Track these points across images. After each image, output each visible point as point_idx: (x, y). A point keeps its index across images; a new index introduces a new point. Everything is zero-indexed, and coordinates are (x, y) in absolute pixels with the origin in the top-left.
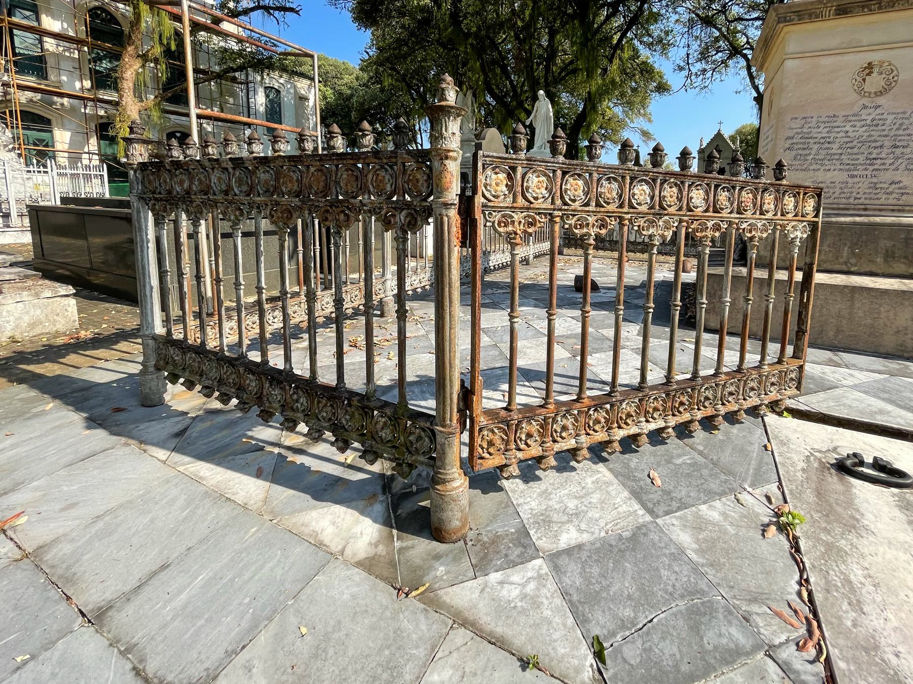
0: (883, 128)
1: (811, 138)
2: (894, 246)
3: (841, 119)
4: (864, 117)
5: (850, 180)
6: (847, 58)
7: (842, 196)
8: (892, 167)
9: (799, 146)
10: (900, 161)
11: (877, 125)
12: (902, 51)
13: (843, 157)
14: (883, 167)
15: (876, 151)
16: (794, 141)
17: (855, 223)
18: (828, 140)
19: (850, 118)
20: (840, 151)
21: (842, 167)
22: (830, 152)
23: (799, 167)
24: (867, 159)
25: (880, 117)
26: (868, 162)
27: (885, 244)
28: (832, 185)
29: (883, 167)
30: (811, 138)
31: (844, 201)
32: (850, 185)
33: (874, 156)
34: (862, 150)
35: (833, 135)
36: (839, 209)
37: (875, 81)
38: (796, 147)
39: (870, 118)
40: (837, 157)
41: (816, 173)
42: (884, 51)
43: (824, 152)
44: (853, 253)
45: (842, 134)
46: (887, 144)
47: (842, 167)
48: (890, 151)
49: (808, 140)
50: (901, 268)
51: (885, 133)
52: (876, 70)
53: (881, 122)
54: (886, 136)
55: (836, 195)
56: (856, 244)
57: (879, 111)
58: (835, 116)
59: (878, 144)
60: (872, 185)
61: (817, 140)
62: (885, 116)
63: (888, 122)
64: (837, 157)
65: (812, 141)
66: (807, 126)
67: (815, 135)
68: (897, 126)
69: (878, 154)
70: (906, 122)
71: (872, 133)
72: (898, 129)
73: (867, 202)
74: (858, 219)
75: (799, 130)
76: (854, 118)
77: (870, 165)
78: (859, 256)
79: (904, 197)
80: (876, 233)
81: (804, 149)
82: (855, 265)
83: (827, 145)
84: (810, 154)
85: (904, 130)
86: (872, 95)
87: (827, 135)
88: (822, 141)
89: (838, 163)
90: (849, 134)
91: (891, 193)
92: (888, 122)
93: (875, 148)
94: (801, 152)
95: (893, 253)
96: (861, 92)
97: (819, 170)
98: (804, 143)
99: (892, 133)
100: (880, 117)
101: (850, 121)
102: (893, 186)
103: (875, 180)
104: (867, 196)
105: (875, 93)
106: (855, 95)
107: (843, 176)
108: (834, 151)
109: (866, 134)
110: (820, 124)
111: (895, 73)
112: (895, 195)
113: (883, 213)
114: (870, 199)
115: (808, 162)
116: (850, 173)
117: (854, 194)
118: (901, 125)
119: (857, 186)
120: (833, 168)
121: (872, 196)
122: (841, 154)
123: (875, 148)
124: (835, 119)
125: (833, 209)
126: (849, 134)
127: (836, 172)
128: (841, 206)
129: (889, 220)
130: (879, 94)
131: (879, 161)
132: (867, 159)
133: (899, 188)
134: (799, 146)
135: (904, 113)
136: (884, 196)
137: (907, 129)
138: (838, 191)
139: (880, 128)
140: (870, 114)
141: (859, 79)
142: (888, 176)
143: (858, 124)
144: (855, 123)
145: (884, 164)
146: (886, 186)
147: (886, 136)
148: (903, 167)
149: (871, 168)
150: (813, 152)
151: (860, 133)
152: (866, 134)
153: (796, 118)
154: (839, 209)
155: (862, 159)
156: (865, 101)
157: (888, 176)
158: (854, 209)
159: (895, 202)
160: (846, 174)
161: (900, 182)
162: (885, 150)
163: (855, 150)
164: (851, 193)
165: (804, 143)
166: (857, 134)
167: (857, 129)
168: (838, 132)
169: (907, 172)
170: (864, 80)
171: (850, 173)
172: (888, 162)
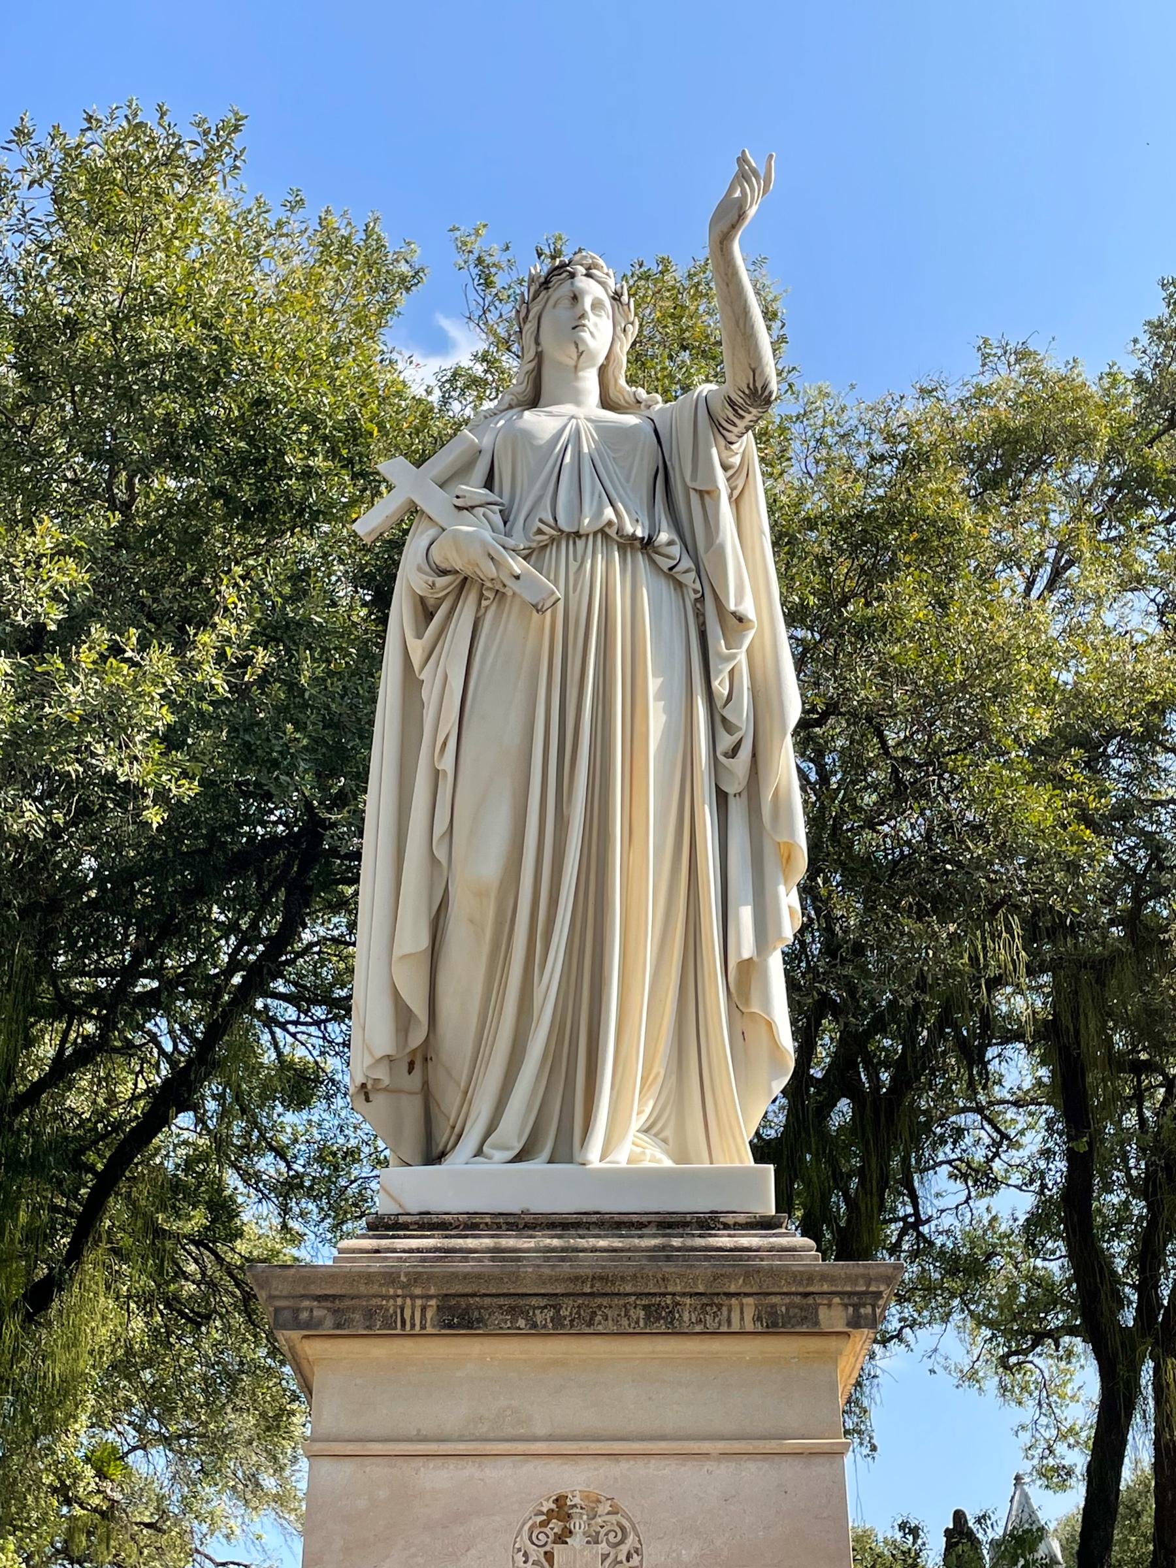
42: (592, 1463)
52: (579, 1524)
111: (631, 1540)
141: (536, 1554)
170: (549, 1556)
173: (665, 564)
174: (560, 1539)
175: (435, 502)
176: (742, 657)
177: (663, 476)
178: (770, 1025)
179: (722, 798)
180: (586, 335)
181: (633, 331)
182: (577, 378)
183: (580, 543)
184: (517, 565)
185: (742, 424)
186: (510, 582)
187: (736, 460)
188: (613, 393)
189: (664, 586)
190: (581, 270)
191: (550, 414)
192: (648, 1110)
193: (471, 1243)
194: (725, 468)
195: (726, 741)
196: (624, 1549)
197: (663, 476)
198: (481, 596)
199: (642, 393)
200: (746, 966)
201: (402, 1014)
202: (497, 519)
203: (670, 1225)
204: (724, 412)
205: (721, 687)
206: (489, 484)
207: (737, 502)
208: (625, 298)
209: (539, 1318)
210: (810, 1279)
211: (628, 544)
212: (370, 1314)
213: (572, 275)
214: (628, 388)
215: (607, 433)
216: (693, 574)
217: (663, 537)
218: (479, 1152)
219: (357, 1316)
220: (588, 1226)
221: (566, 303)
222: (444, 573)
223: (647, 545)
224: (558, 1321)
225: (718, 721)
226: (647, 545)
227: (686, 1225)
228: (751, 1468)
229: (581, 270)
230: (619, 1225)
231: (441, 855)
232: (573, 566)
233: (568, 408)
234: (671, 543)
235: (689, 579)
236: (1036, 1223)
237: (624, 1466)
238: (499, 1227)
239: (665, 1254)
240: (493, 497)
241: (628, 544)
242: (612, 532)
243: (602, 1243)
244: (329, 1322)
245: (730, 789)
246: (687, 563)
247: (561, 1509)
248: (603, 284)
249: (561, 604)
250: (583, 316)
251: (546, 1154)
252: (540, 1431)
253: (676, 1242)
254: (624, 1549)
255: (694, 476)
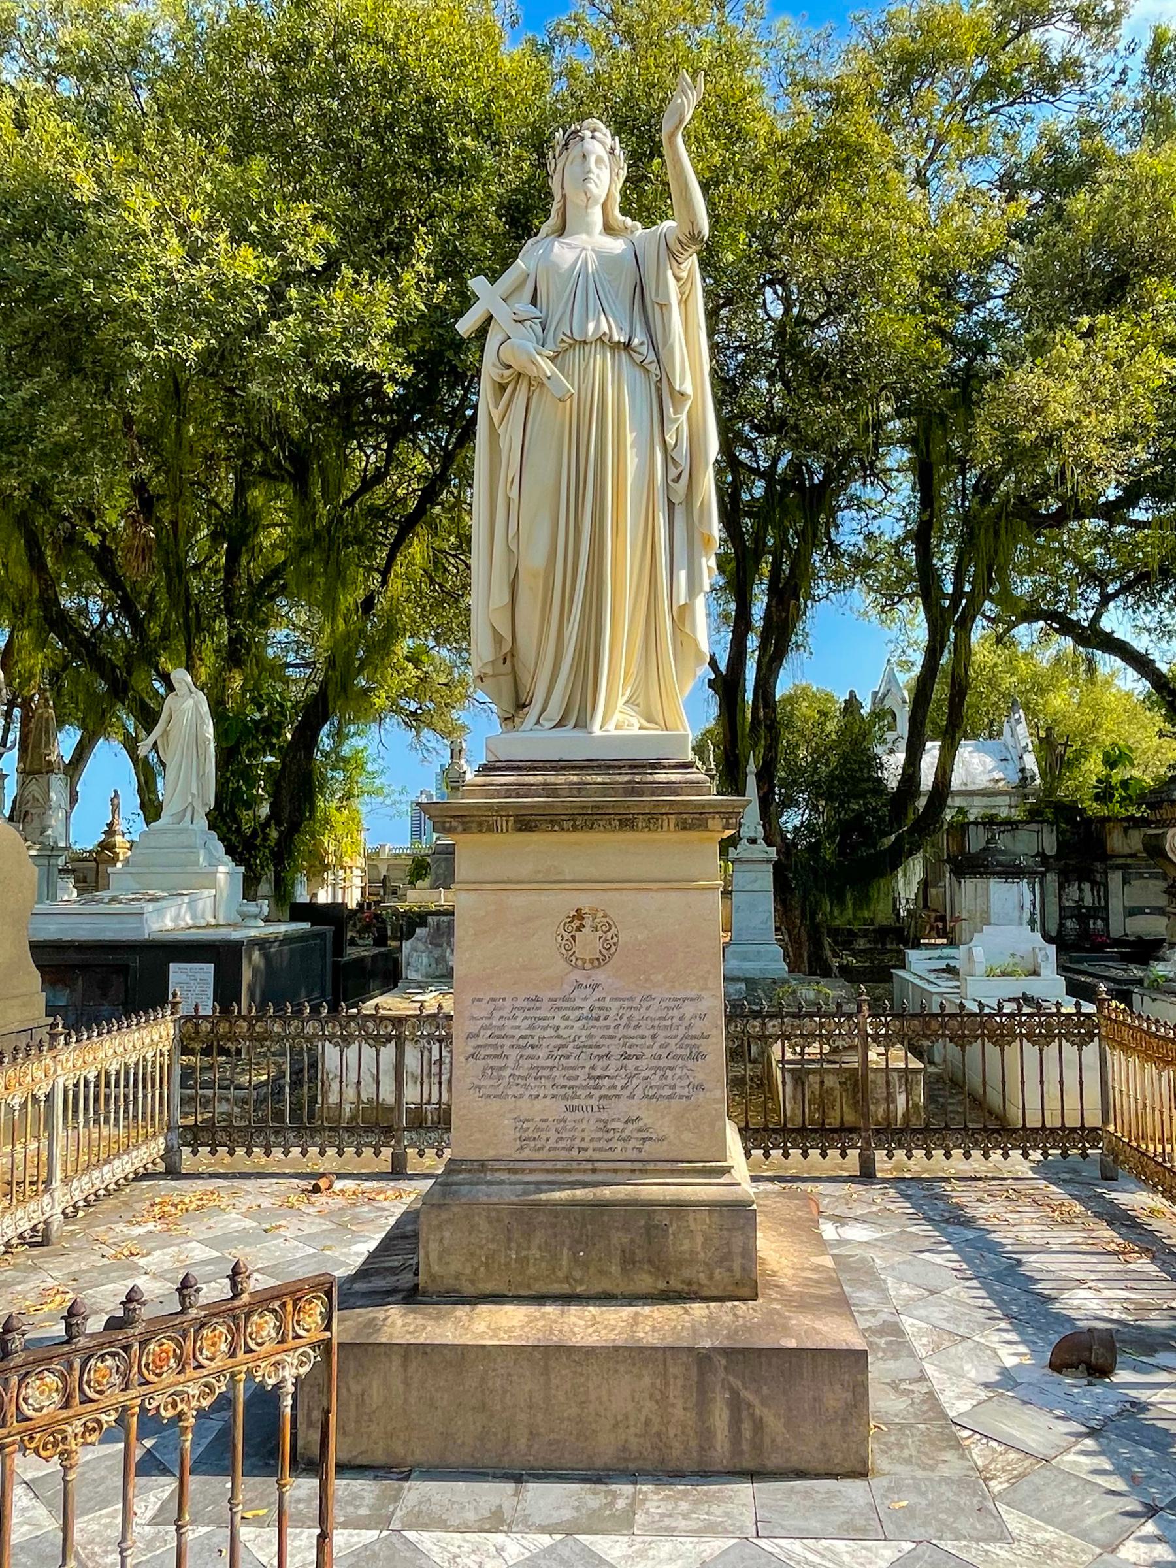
0: (607, 1023)
1: (505, 1037)
2: (632, 1241)
3: (546, 1004)
4: (578, 1003)
5: (570, 1116)
6: (544, 898)
7: (561, 1144)
8: (627, 1092)
9: (489, 1052)
10: (635, 1081)
11: (597, 1019)
12: (617, 894)
13: (556, 1073)
14: (613, 1092)
15: (600, 1064)
16: (480, 1041)
17: (573, 1203)
18: (531, 1042)
19: (560, 1004)
20: (550, 1063)
21: (555, 1092)
22: (536, 1063)
23: (492, 1092)
24: (590, 1077)
25: (601, 1004)
26: (592, 1082)
27: (618, 1238)
28: (544, 1125)
29: (613, 1092)
30: (505, 1037)
31: (563, 1154)
32: (570, 1125)
33: (598, 1072)
34: (581, 1063)
35: (537, 1033)
36: (557, 1171)
37: (589, 942)
38: (484, 1052)
39: (587, 1004)
40: (546, 1073)
41: (519, 1102)
43: (526, 1064)
44: (575, 1257)
45: (550, 1032)
46: (616, 1051)
47: (555, 1092)
48: (620, 1063)
49: (501, 1042)
50: (645, 1282)
51: (611, 1032)
52: (587, 922)
53: (603, 1013)
54: (612, 1037)
55: (551, 1143)
56: (579, 1242)
57: (598, 994)
58: (537, 999)
59: (603, 1051)
60: (602, 1125)
61: (514, 1041)
62: (607, 1003)
63: (612, 1013)
64: (546, 1073)
65: (507, 1042)
66: (497, 1014)
67: (512, 1032)
68: (624, 1021)
69: (605, 1069)
70: (636, 1014)
71: (593, 1031)
72: (627, 1026)
73: (597, 1155)
74: (580, 1193)
75: (487, 1022)
76: (565, 1004)
77: (596, 1087)
78: (585, 1265)
79: (647, 1145)
80: (606, 1218)
81: (496, 1057)
82: (580, 1282)
83: (530, 1051)
84: (504, 1068)
85: (636, 1027)
86: (587, 966)
87: (528, 1032)
88: (522, 1042)
89: (549, 1084)
90: (561, 1032)
91: (627, 1140)
92: (612, 1013)
93: (600, 1058)
94: (491, 1062)
95: (633, 1253)
96: (570, 958)
97: (522, 1096)
98: (495, 1046)
99: (621, 1032)
100: (601, 1004)
101: (560, 1009)
102: (630, 1126)
103: (604, 1116)
104: (596, 1145)
105: (592, 961)
106: (562, 963)
107: (556, 1109)
108: (541, 1063)
109: (584, 1033)
110: (518, 1013)
111: (613, 930)
112: (633, 1143)
113: (619, 1178)
114: (601, 1150)
115: (505, 1082)
116: (568, 1103)
117: (577, 1142)
118: (630, 1018)
119: (580, 1127)
120: (542, 1092)
121: (603, 1144)
122: (552, 1068)
123: (600, 1058)
124: (538, 1004)
125: (548, 1171)
126: (561, 1032)
127: (548, 1101)
128: (559, 1165)
129: (622, 1192)
130: (600, 962)
131: (606, 1082)
132: (590, 1077)
133: (640, 1130)
134: (489, 1052)
135: (632, 999)
136: (620, 1145)
137: (636, 1027)
138: (553, 1136)
139: (602, 1023)
140: (586, 999)
141: (567, 936)
142: (621, 1108)
143: (573, 1015)
144: (569, 1013)
145: (614, 1087)
146: (620, 1126)
147: (612, 1037)
148: (639, 1093)
149: (597, 1093)
150: (511, 1063)
151: (575, 1031)
152: (584, 1033)
153: (480, 1000)
154: (557, 1171)
155: (582, 1077)
156: (577, 975)
157: (621, 1108)
158: (578, 1171)
159: (634, 1155)
160: (563, 1103)
161: (638, 1119)
162: (614, 1063)
163: (572, 1061)
164: (573, 1139)
165: (495, 1046)
166: (573, 1033)
167: (569, 1023)
168: (545, 1028)
169: (645, 1101)
171: (568, 1103)
172: (620, 1083)
173: (638, 358)
174: (579, 929)
175: (503, 315)
176: (683, 417)
177: (640, 287)
178: (695, 641)
179: (671, 505)
180: (591, 186)
181: (623, 174)
182: (587, 214)
183: (587, 348)
184: (548, 367)
185: (686, 254)
186: (545, 381)
187: (684, 275)
188: (611, 221)
189: (638, 372)
190: (588, 134)
191: (571, 247)
192: (628, 693)
193: (531, 779)
194: (678, 279)
195: (674, 472)
196: (609, 935)
197: (640, 287)
198: (530, 384)
199: (628, 220)
200: (682, 608)
201: (498, 638)
202: (538, 329)
203: (635, 767)
204: (676, 247)
205: (671, 440)
206: (534, 302)
207: (684, 302)
208: (617, 152)
209: (565, 825)
210: (703, 806)
211: (615, 346)
212: (480, 824)
213: (583, 139)
214: (621, 218)
215: (607, 261)
216: (655, 365)
217: (636, 342)
218: (538, 722)
219: (474, 825)
220: (592, 767)
221: (579, 160)
222: (509, 367)
223: (627, 346)
224: (575, 828)
225: (669, 459)
226: (627, 346)
227: (643, 767)
228: (673, 896)
229: (588, 134)
230: (609, 767)
231: (514, 548)
232: (583, 364)
233: (584, 236)
234: (642, 344)
235: (653, 368)
236: (902, 541)
237: (610, 893)
238: (547, 769)
239: (632, 789)
240: (536, 312)
241: (615, 346)
242: (606, 339)
243: (599, 779)
244: (460, 828)
245: (676, 501)
246: (652, 357)
247: (579, 915)
248: (603, 144)
249: (575, 397)
250: (589, 172)
251: (572, 722)
252: (568, 878)
253: (638, 778)
254: (609, 935)
255: (657, 295)
